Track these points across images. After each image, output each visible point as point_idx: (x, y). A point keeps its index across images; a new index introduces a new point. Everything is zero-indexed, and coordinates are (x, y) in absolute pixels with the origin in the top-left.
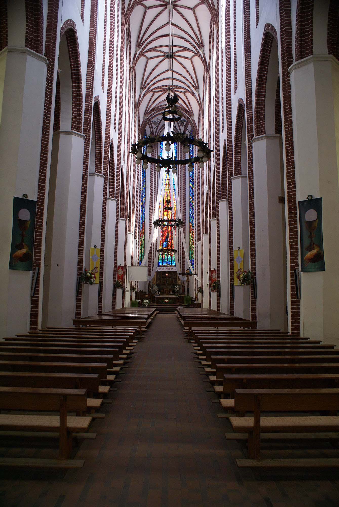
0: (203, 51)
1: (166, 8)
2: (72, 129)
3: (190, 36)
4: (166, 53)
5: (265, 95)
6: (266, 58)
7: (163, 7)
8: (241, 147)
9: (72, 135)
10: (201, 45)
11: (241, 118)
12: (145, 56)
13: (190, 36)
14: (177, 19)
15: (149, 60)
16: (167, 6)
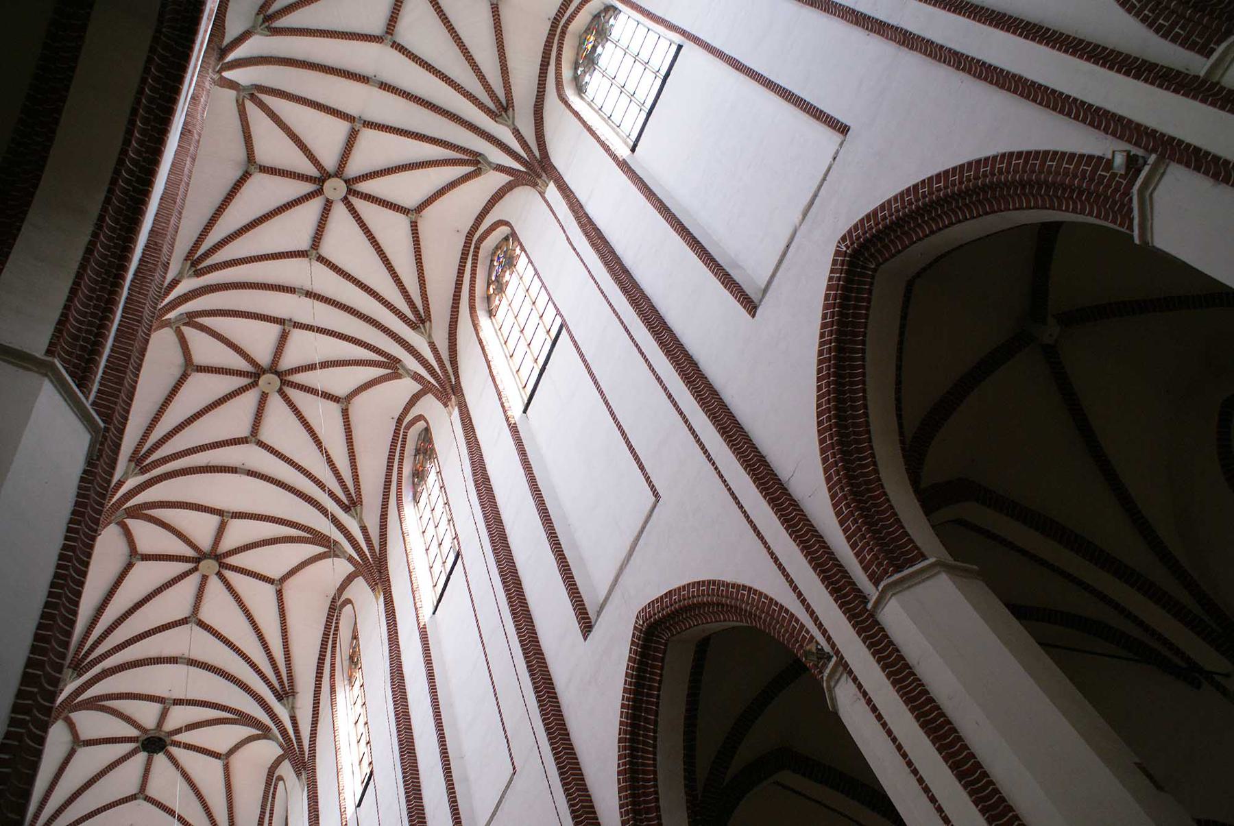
0: (293, 708)
1: (195, 569)
2: (49, 352)
3: (253, 666)
4: (148, 730)
5: (871, 448)
6: (855, 334)
7: (188, 566)
8: (658, 809)
9: (46, 375)
10: (286, 693)
11: (651, 688)
12: (71, 726)
13: (253, 666)
14: (218, 610)
15: (80, 746)
16: (199, 562)
